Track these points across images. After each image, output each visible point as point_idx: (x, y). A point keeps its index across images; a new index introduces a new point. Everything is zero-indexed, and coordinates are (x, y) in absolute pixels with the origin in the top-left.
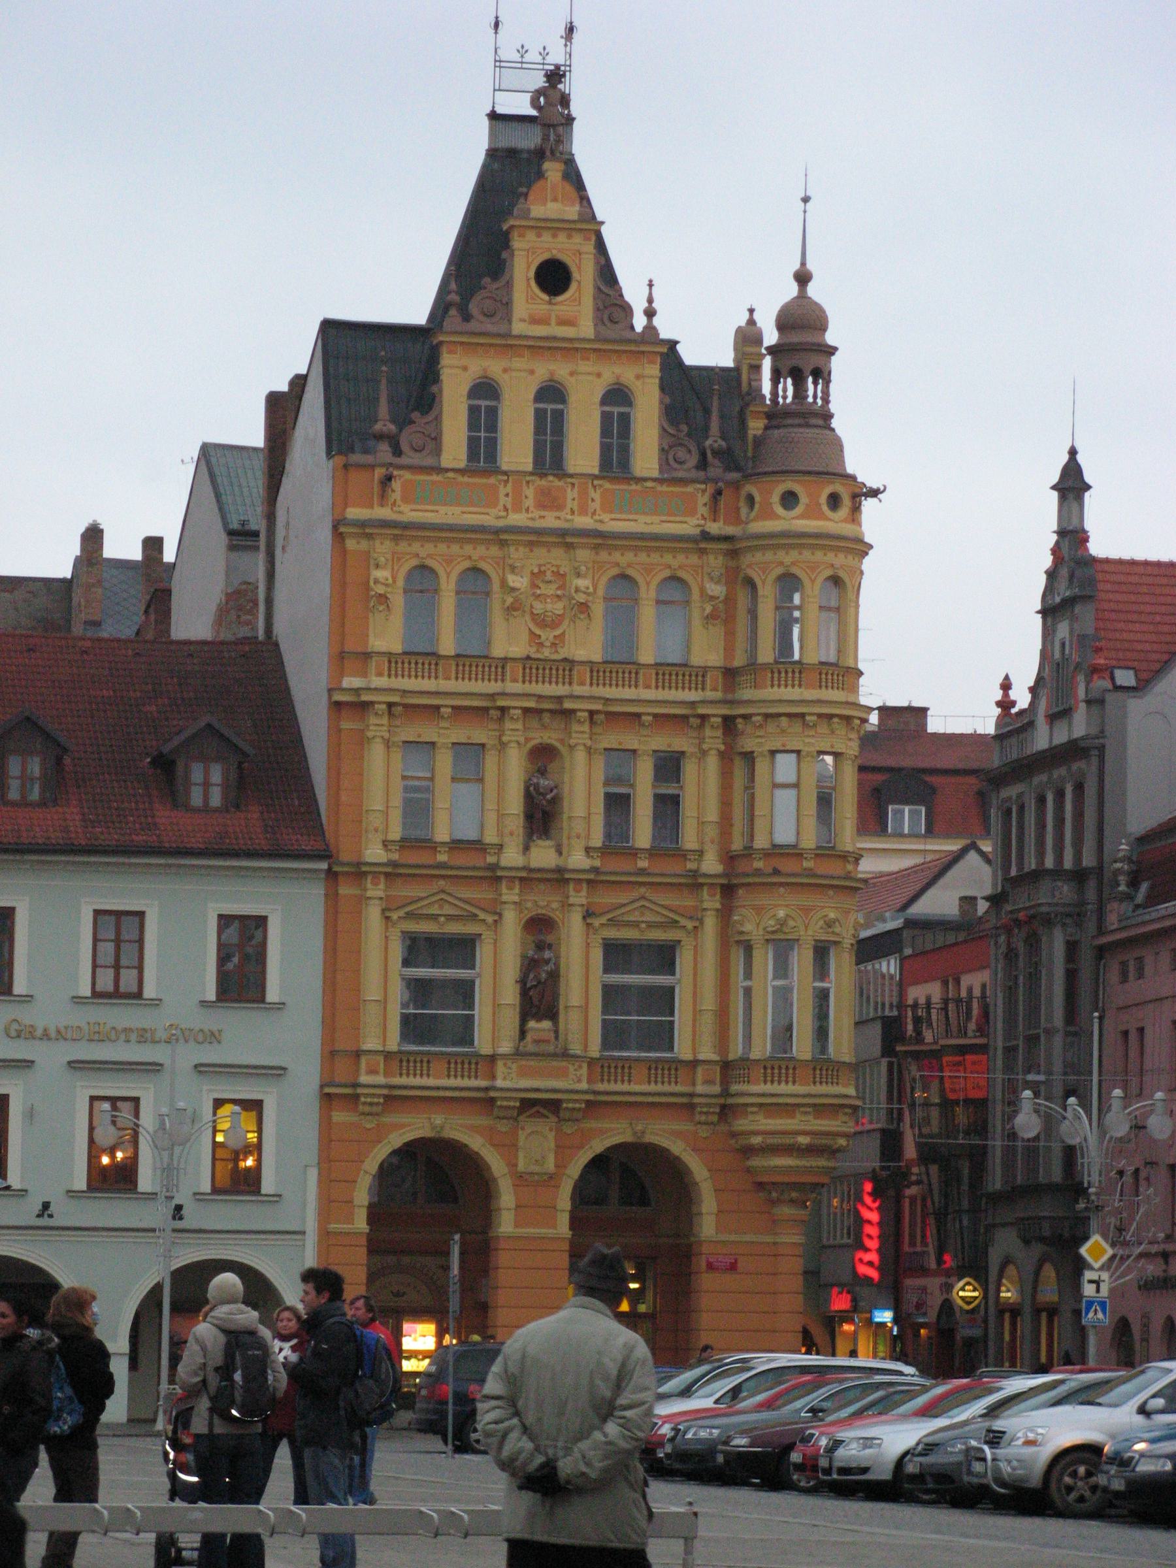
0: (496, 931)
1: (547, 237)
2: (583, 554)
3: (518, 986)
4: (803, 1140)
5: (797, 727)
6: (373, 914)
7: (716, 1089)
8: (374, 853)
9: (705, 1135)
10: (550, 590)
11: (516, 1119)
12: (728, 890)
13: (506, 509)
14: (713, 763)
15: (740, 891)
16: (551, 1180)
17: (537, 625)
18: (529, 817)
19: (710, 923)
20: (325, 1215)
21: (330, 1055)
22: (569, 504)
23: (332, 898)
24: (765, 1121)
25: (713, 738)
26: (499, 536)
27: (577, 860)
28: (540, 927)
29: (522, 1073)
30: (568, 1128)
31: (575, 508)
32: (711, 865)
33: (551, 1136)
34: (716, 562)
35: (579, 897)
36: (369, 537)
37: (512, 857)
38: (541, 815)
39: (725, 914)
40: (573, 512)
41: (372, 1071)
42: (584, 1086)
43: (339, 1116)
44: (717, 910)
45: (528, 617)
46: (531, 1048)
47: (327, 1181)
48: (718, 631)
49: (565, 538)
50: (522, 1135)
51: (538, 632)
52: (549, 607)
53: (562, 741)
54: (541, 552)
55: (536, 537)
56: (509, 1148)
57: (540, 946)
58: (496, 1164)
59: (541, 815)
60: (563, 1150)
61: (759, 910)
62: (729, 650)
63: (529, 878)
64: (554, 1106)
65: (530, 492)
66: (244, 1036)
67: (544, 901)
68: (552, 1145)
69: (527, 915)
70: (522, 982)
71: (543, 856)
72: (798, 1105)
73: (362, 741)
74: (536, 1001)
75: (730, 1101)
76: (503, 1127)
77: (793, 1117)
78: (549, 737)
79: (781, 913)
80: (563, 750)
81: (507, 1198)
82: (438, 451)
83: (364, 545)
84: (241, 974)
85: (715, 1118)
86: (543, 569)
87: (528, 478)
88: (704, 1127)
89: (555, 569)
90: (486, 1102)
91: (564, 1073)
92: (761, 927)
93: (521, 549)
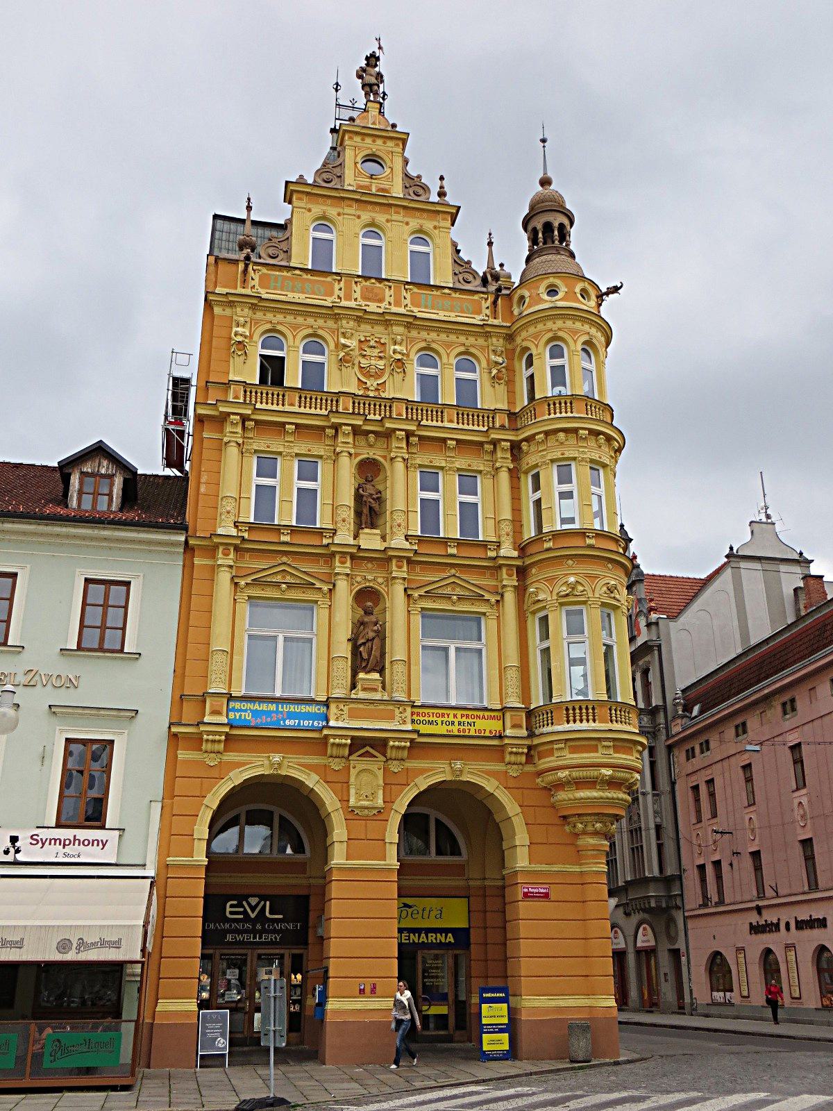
0: (330, 599)
1: (369, 140)
2: (400, 329)
3: (350, 644)
4: (607, 772)
5: (572, 440)
6: (224, 577)
8: (226, 529)
9: (515, 775)
10: (376, 352)
11: (347, 758)
12: (522, 572)
13: (339, 298)
14: (504, 476)
15: (534, 571)
16: (380, 815)
17: (364, 375)
18: (358, 514)
19: (510, 597)
20: (165, 848)
21: (180, 699)
22: (387, 299)
23: (189, 568)
25: (504, 459)
26: (333, 313)
27: (398, 542)
29: (352, 715)
30: (395, 767)
31: (392, 301)
32: (508, 550)
33: (380, 774)
34: (498, 343)
35: (400, 572)
36: (231, 304)
37: (345, 536)
38: (369, 511)
39: (521, 591)
40: (390, 304)
41: (216, 712)
42: (409, 727)
43: (182, 755)
45: (356, 368)
46: (362, 695)
47: (168, 814)
48: (502, 389)
49: (385, 320)
50: (353, 772)
51: (364, 380)
52: (373, 362)
53: (385, 457)
54: (364, 327)
55: (362, 317)
56: (341, 785)
57: (368, 612)
58: (328, 798)
59: (369, 511)
60: (392, 785)
61: (551, 580)
62: (511, 402)
63: (357, 557)
64: (380, 745)
65: (358, 289)
66: (100, 683)
67: (371, 577)
68: (381, 782)
70: (353, 640)
71: (370, 540)
72: (599, 739)
73: (221, 446)
74: (365, 656)
75: (536, 741)
76: (336, 765)
77: (597, 751)
78: (376, 454)
79: (572, 579)
80: (386, 464)
81: (339, 832)
82: (289, 259)
83: (228, 312)
84: (101, 632)
85: (523, 759)
86: (368, 339)
87: (356, 280)
89: (377, 340)
90: (320, 744)
92: (555, 593)
93: (352, 323)
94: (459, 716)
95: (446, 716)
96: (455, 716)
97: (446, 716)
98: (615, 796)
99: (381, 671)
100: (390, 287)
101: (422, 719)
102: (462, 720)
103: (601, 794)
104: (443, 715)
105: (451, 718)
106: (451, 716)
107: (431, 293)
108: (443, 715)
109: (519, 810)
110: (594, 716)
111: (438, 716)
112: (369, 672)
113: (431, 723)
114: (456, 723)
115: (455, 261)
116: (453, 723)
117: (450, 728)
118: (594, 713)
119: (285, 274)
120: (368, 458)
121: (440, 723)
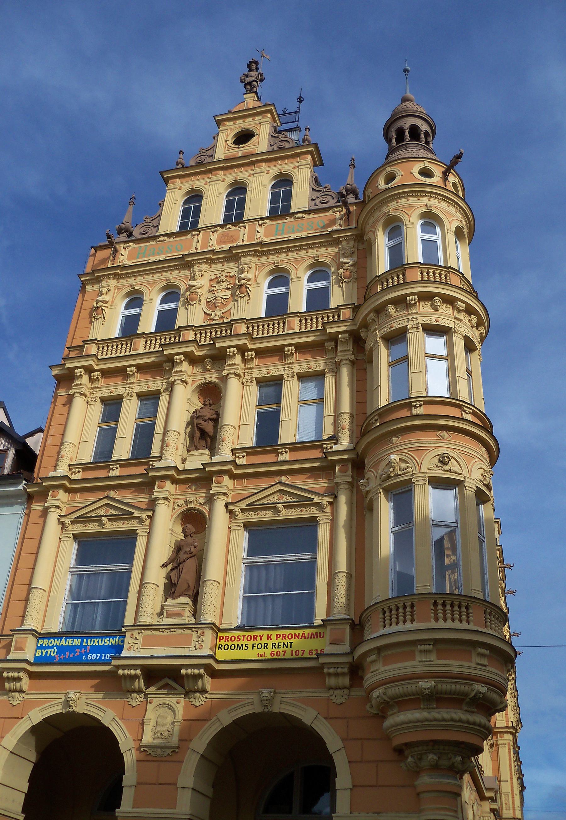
4: (426, 684)
7: (346, 648)
9: (338, 701)
24: (383, 669)
28: (195, 522)
29: (147, 644)
44: (349, 483)
69: (179, 511)
77: (414, 659)
78: (212, 377)
83: (96, 287)
85: (346, 681)
86: (218, 276)
88: (337, 692)
91: (187, 642)
94: (273, 637)
95: (259, 638)
96: (269, 637)
97: (259, 638)
98: (446, 716)
99: (196, 598)
100: (245, 227)
101: (230, 643)
102: (277, 642)
103: (425, 714)
104: (255, 638)
105: (264, 640)
106: (265, 638)
107: (286, 221)
108: (255, 638)
109: (340, 744)
110: (412, 616)
111: (249, 638)
112: (178, 597)
113: (240, 647)
114: (270, 646)
115: (313, 189)
116: (266, 646)
117: (262, 651)
118: (412, 612)
119: (151, 243)
120: (205, 383)
121: (250, 646)
